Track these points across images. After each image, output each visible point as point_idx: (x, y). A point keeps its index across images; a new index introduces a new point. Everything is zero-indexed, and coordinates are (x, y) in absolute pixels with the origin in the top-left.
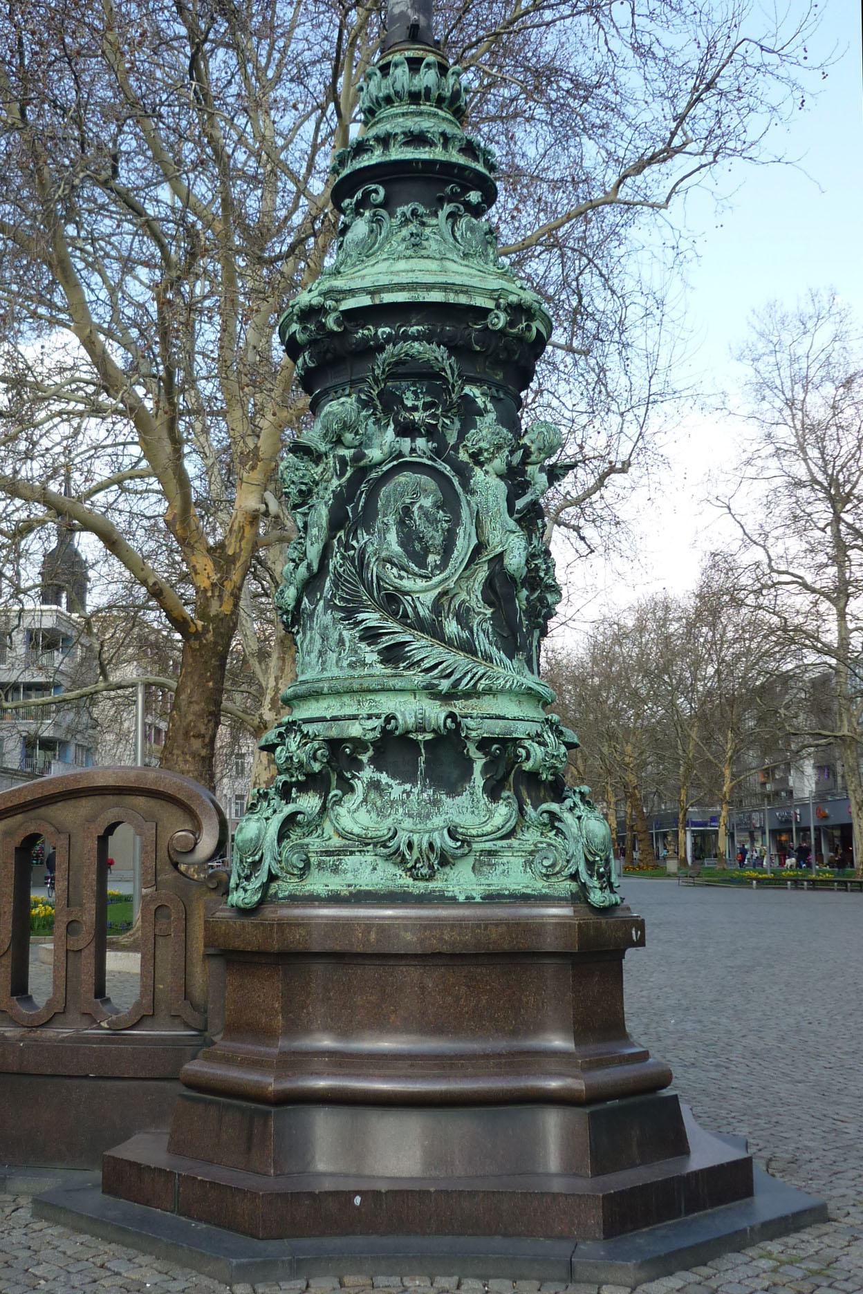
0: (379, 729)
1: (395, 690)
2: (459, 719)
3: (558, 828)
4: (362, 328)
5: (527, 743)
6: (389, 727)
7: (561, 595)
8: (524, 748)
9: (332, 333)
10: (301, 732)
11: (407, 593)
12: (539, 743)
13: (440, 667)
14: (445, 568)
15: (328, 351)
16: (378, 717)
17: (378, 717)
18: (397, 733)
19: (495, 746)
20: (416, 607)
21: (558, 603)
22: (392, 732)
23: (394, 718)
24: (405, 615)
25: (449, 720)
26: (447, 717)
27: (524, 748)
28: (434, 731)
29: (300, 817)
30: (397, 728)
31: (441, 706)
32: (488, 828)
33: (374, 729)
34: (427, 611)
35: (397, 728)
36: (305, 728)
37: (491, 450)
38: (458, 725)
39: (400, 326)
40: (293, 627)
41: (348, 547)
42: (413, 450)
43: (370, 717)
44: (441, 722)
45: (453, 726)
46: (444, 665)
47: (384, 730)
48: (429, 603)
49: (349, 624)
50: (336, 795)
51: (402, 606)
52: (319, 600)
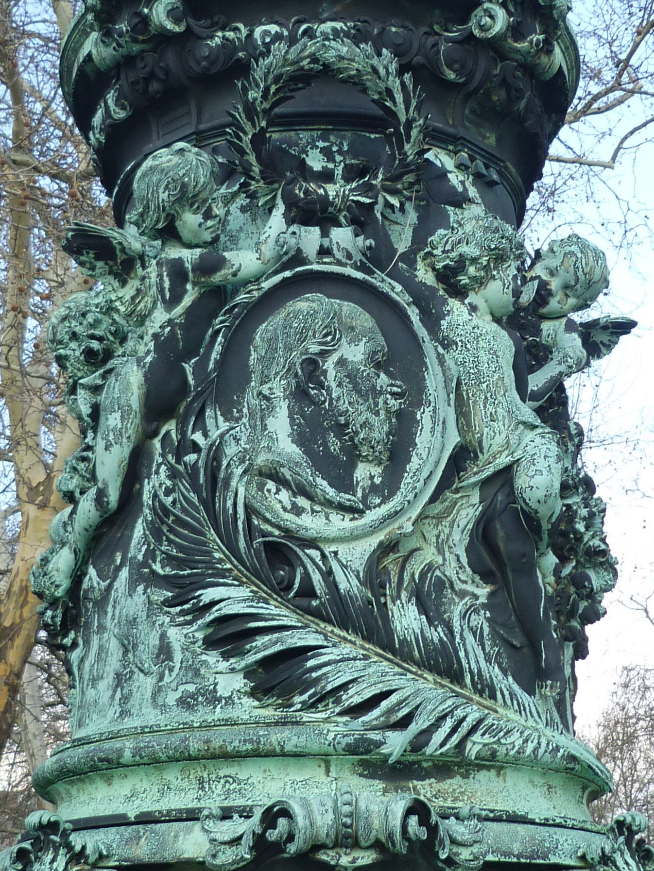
0: (248, 841)
1: (284, 755)
2: (434, 818)
4: (223, 29)
6: (273, 835)
7: (615, 574)
9: (164, 38)
10: (69, 847)
11: (312, 543)
13: (385, 704)
14: (392, 493)
15: (152, 75)
16: (246, 813)
17: (246, 813)
18: (292, 848)
21: (608, 588)
22: (278, 847)
23: (286, 813)
24: (308, 591)
25: (413, 820)
26: (409, 812)
28: (377, 845)
30: (291, 838)
31: (385, 791)
33: (236, 841)
34: (355, 582)
36: (77, 840)
37: (484, 261)
38: (433, 830)
39: (300, 22)
40: (65, 635)
41: (186, 446)
42: (324, 252)
43: (226, 814)
44: (398, 823)
46: (393, 699)
47: (260, 842)
48: (359, 564)
49: (183, 613)
51: (299, 571)
52: (118, 569)
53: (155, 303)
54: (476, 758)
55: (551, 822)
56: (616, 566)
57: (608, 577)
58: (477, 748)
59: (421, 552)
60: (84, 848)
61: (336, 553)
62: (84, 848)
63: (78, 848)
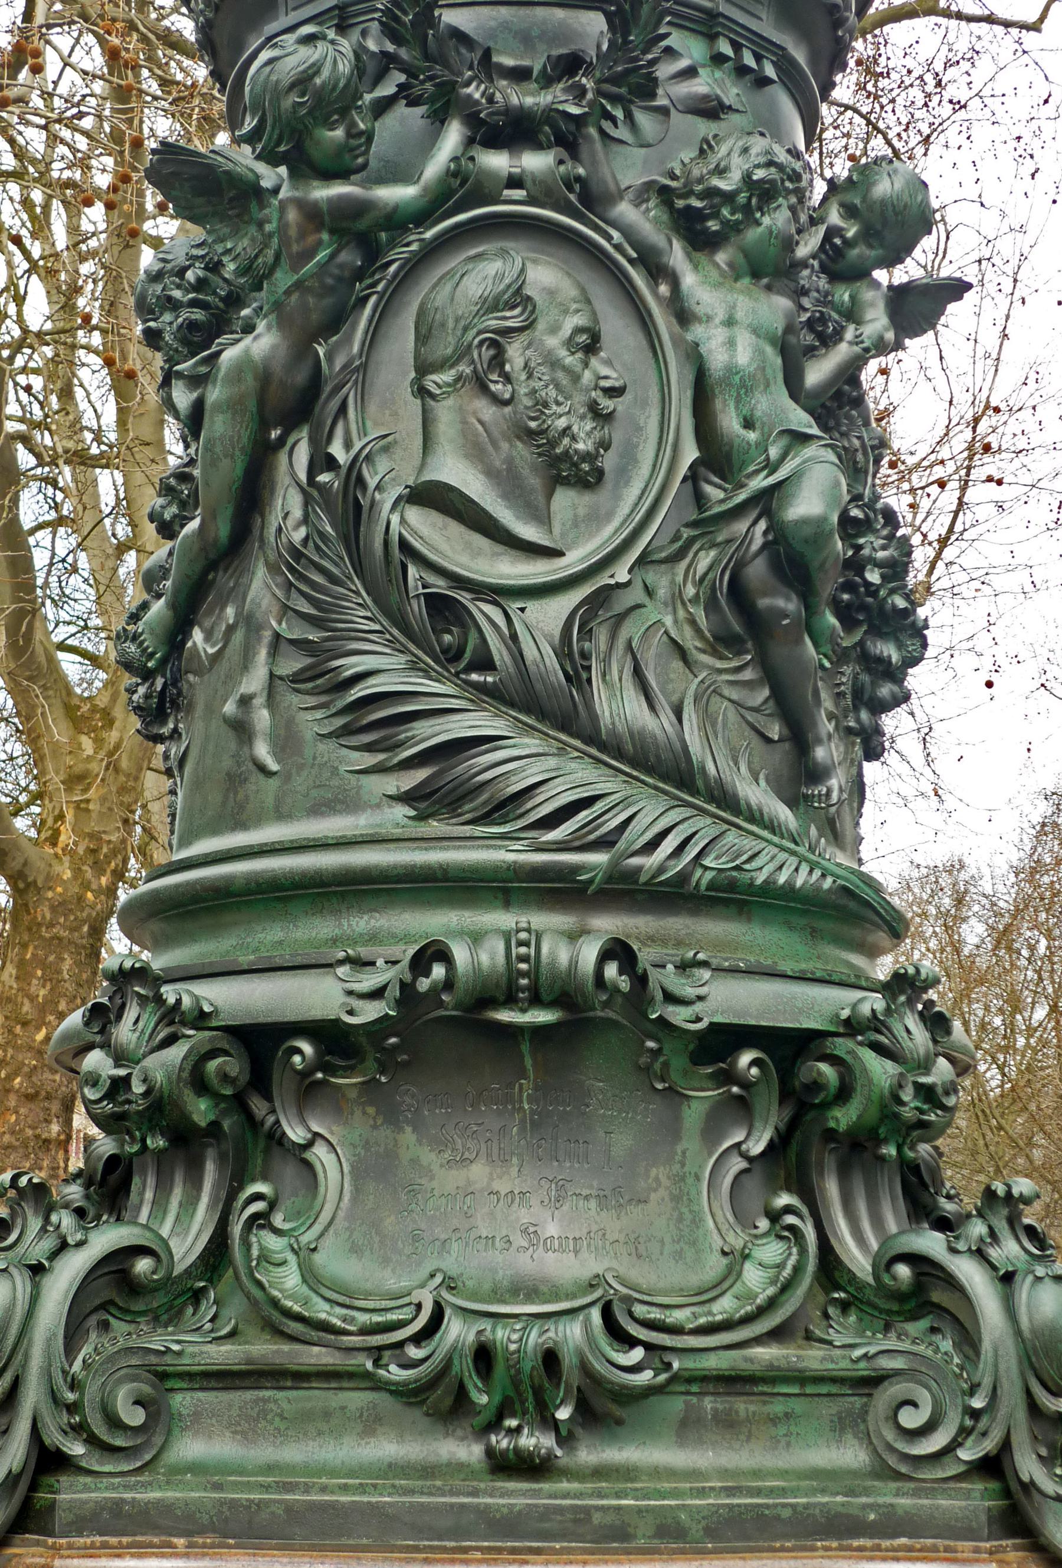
0: (394, 992)
3: (940, 1310)
5: (842, 1046)
7: (925, 645)
8: (834, 1060)
10: (159, 1000)
12: (878, 1049)
13: (584, 816)
19: (745, 1058)
20: (514, 637)
21: (915, 661)
23: (443, 955)
24: (485, 663)
26: (605, 956)
27: (834, 1060)
29: (143, 1265)
32: (725, 1307)
33: (377, 994)
34: (547, 650)
35: (449, 984)
36: (169, 993)
37: (742, 198)
38: (641, 981)
40: (164, 722)
41: (322, 461)
45: (624, 984)
46: (599, 807)
48: (555, 628)
50: (258, 1197)
53: (277, 257)
54: (707, 889)
55: (809, 976)
56: (925, 632)
57: (912, 645)
58: (709, 875)
59: (643, 610)
60: (179, 1001)
61: (522, 610)
62: (179, 1001)
63: (171, 1000)
